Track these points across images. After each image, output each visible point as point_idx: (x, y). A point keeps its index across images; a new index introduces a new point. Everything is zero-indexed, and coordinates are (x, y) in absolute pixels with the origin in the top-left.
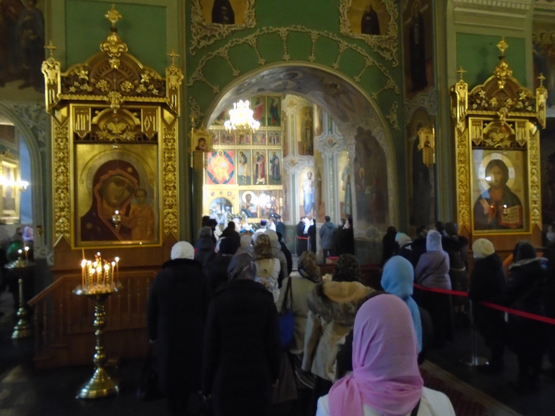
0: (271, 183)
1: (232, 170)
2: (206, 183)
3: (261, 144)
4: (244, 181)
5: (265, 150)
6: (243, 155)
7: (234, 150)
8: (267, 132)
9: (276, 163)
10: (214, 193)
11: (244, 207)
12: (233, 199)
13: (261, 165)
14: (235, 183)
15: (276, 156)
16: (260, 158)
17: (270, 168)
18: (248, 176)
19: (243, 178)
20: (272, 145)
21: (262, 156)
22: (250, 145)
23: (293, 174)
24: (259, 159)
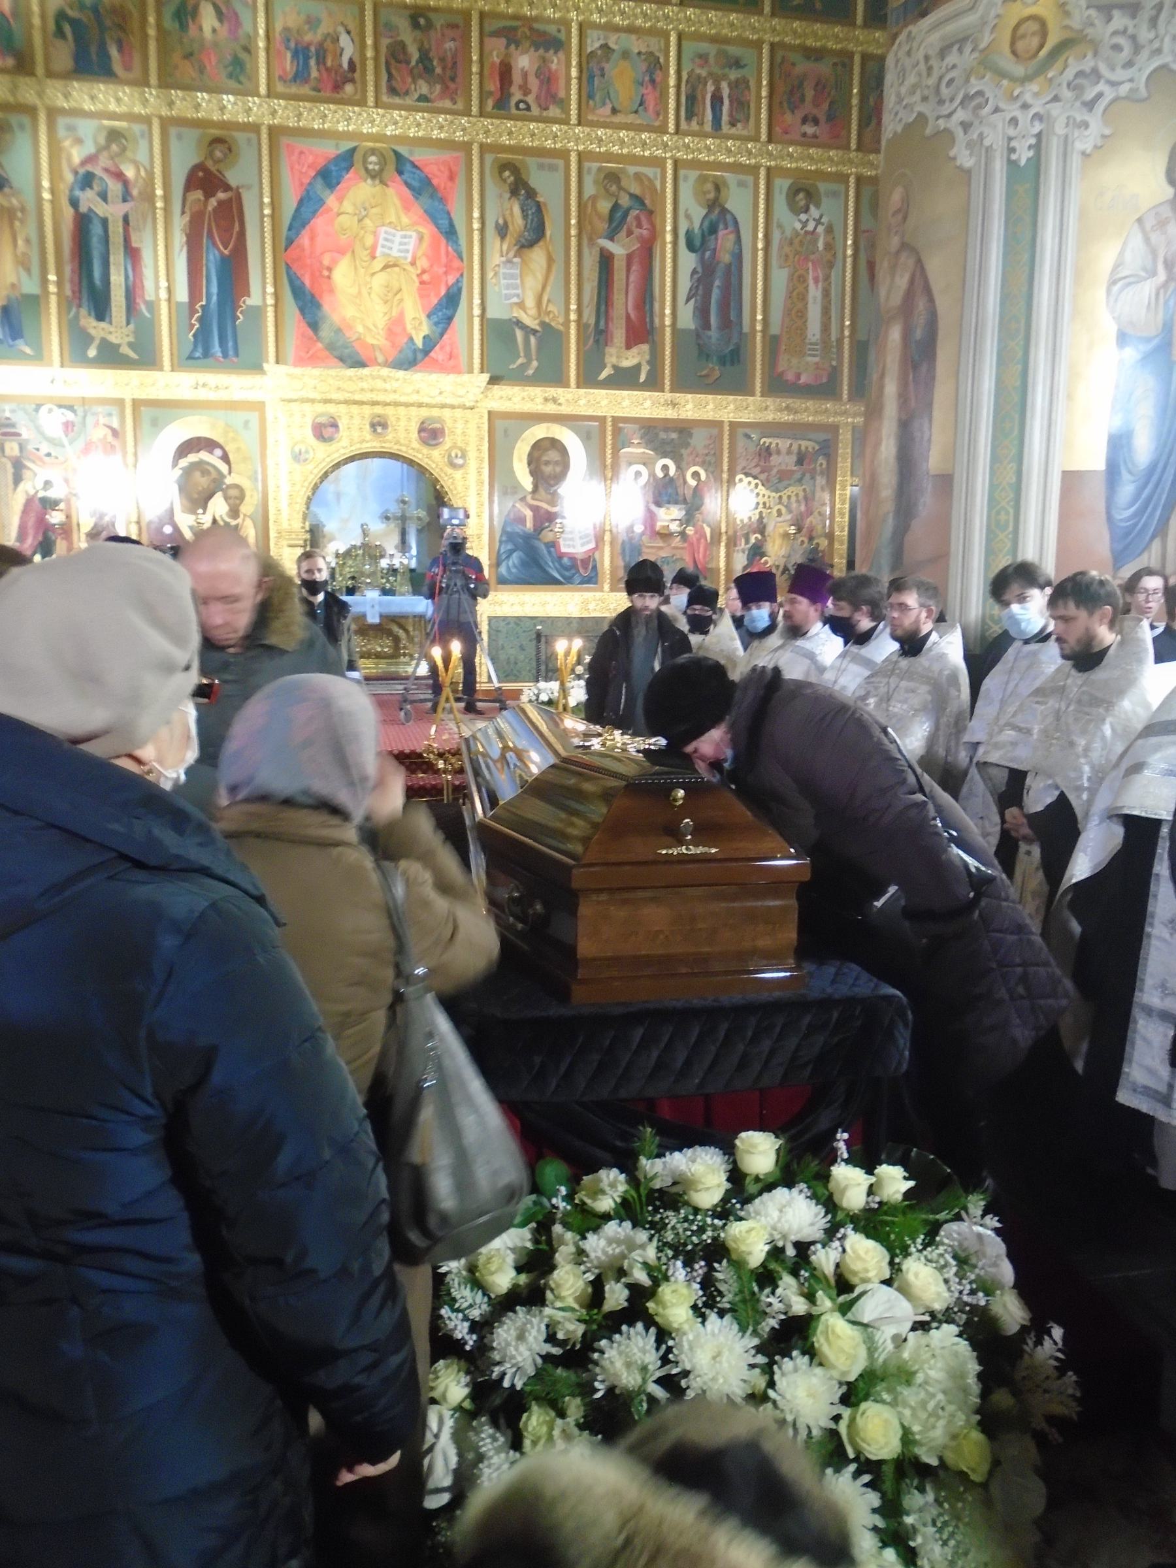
0: (683, 384)
1: (451, 280)
2: (277, 362)
3: (631, 119)
4: (520, 361)
5: (659, 163)
6: (520, 188)
7: (466, 147)
8: (673, 39)
9: (726, 258)
10: (335, 425)
11: (522, 520)
12: (453, 465)
13: (629, 258)
14: (471, 371)
15: (724, 211)
16: (626, 213)
17: (685, 284)
18: (543, 324)
19: (519, 334)
20: (707, 136)
21: (638, 199)
22: (566, 122)
23: (1024, 155)
24: (616, 222)
